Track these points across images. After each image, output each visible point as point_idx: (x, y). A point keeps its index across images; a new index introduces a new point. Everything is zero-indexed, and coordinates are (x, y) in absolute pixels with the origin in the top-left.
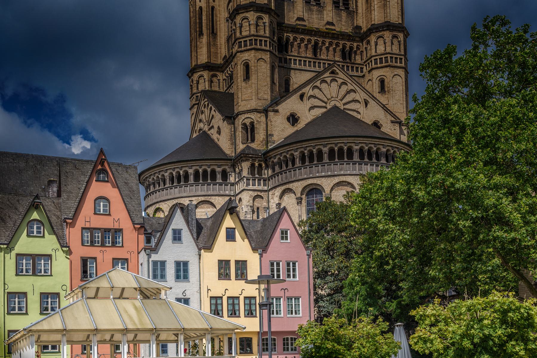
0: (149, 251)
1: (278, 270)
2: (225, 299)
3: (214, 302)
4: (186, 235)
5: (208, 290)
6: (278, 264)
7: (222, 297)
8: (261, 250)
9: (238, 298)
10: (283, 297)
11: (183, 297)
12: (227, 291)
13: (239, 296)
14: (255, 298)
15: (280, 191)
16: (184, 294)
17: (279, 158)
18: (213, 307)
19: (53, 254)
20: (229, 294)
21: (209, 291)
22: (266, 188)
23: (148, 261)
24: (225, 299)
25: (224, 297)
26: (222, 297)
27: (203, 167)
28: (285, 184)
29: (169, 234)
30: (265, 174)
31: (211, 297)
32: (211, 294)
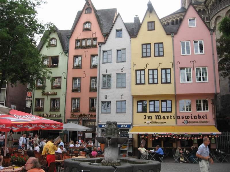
0: (100, 44)
1: (188, 48)
2: (147, 70)
3: (138, 72)
4: (125, 33)
5: (134, 65)
6: (188, 44)
7: (144, 70)
8: (173, 34)
9: (157, 69)
10: (193, 67)
11: (121, 72)
12: (148, 65)
13: (157, 68)
14: (170, 69)
15: (214, 20)
16: (122, 71)
17: (213, 2)
18: (138, 77)
19: (60, 55)
20: (149, 67)
21: (135, 66)
22: (208, 21)
23: (100, 51)
24: (147, 70)
25: (146, 70)
26: (144, 70)
27: (175, 18)
28: (216, 14)
29: (113, 32)
30: (207, 14)
31: (136, 70)
32: (136, 68)
